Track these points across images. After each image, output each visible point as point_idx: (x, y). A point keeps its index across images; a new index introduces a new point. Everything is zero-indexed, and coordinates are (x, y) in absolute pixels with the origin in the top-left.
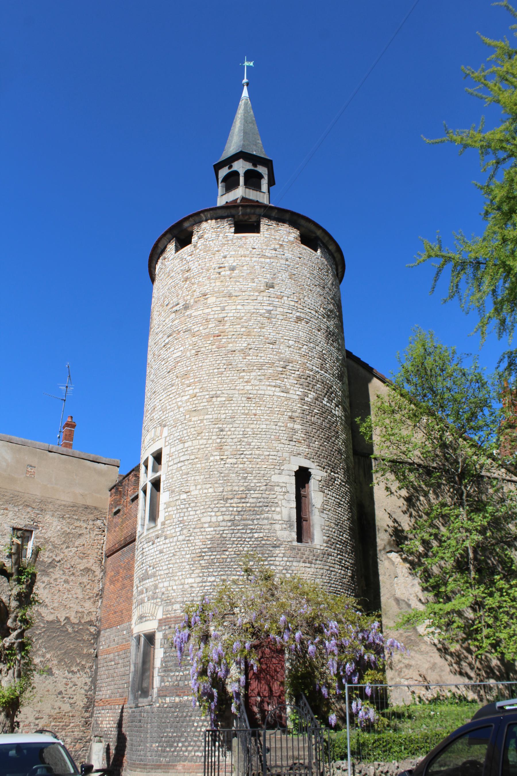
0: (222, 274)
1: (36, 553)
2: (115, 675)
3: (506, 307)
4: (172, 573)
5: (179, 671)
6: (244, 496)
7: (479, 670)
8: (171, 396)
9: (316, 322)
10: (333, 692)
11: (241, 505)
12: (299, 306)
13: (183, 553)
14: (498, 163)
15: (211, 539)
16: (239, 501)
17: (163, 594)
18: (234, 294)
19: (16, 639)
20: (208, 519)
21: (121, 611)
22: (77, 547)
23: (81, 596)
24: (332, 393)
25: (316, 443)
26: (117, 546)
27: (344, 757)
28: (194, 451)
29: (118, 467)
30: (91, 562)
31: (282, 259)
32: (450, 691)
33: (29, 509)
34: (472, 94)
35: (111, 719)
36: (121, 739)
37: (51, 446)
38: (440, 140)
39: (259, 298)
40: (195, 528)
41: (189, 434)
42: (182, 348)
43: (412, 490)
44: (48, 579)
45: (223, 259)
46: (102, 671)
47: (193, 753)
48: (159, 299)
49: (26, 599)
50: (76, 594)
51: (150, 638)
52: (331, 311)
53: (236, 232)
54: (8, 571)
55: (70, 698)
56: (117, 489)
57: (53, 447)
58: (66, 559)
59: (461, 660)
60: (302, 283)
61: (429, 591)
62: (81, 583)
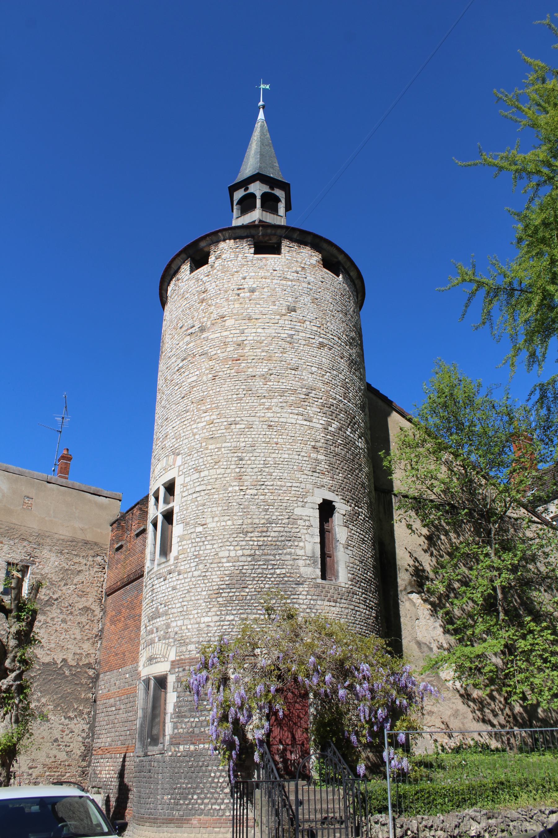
0: (241, 295)
1: (36, 588)
2: (116, 721)
3: (537, 340)
4: (185, 610)
5: (194, 717)
6: (265, 529)
7: (509, 717)
8: (185, 423)
9: (339, 349)
10: (364, 740)
11: (262, 539)
12: (322, 332)
13: (199, 590)
14: (538, 185)
15: (230, 575)
16: (260, 535)
17: (176, 633)
18: (254, 317)
19: (15, 680)
20: (226, 554)
21: (124, 653)
22: (76, 585)
23: (79, 637)
24: (355, 424)
25: (340, 475)
26: (119, 583)
27: (383, 810)
28: (211, 481)
29: (120, 500)
30: (90, 601)
31: (304, 282)
32: (473, 739)
33: (25, 543)
34: (506, 117)
35: (112, 768)
36: (124, 791)
37: (51, 477)
38: (472, 162)
39: (280, 321)
41: (206, 463)
42: (198, 373)
43: (433, 529)
44: (45, 618)
45: (243, 281)
46: (101, 717)
47: (210, 806)
48: (171, 322)
49: (25, 638)
50: (74, 634)
51: (161, 682)
52: (353, 339)
53: (256, 253)
54: (7, 607)
55: (66, 746)
56: (119, 524)
57: (51, 478)
58: (64, 597)
59: (483, 707)
60: (325, 308)
61: (452, 635)
62: (79, 623)
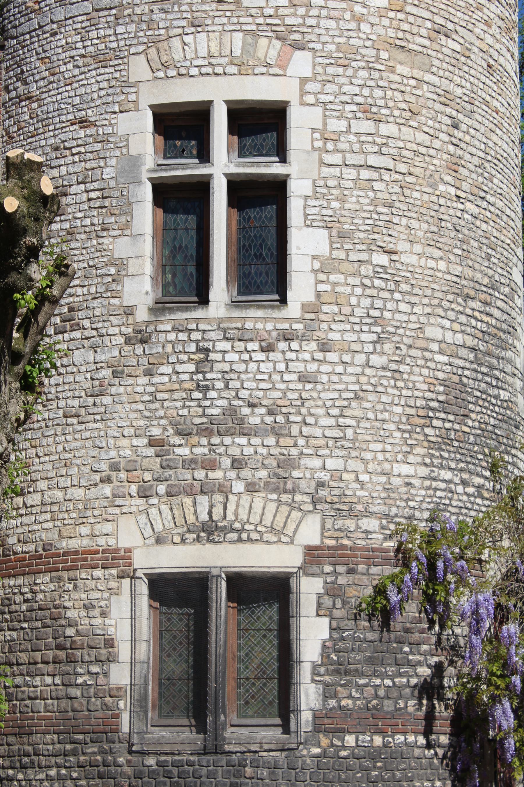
5: (383, 677)
28: (405, 153)
40: (410, 347)
